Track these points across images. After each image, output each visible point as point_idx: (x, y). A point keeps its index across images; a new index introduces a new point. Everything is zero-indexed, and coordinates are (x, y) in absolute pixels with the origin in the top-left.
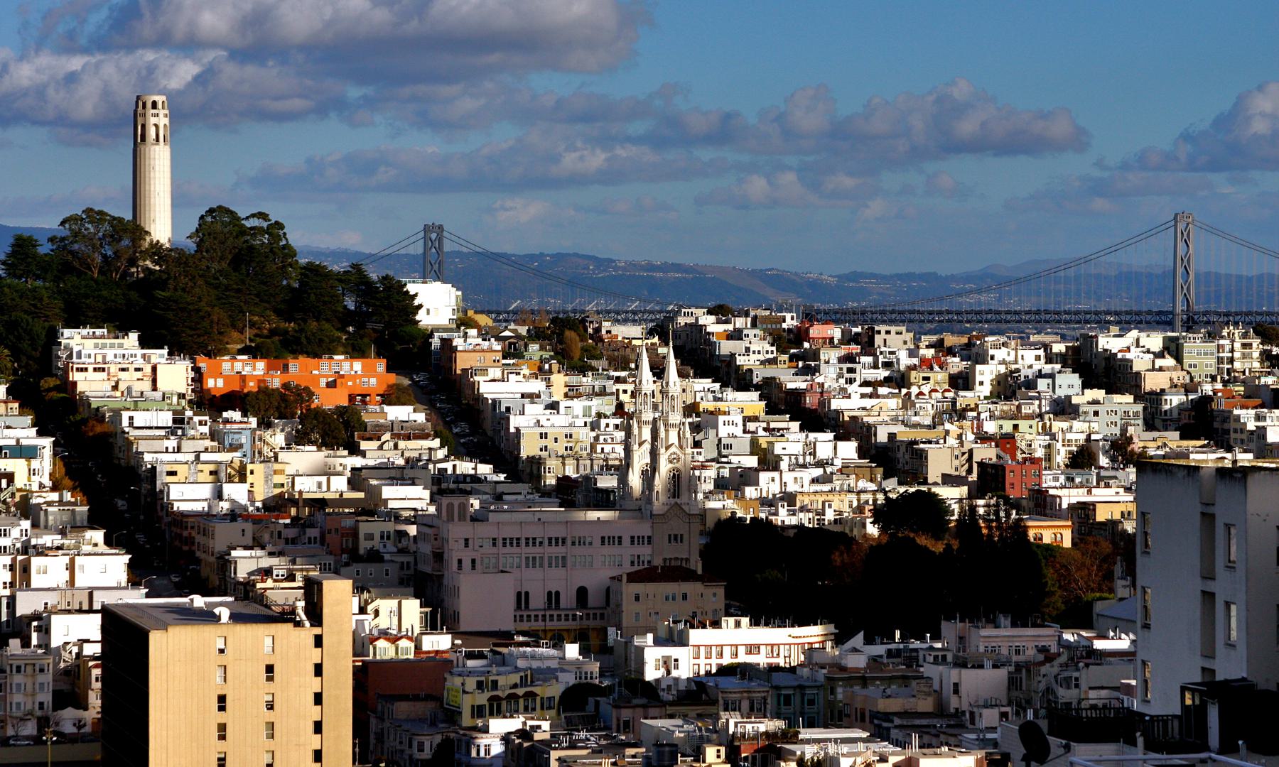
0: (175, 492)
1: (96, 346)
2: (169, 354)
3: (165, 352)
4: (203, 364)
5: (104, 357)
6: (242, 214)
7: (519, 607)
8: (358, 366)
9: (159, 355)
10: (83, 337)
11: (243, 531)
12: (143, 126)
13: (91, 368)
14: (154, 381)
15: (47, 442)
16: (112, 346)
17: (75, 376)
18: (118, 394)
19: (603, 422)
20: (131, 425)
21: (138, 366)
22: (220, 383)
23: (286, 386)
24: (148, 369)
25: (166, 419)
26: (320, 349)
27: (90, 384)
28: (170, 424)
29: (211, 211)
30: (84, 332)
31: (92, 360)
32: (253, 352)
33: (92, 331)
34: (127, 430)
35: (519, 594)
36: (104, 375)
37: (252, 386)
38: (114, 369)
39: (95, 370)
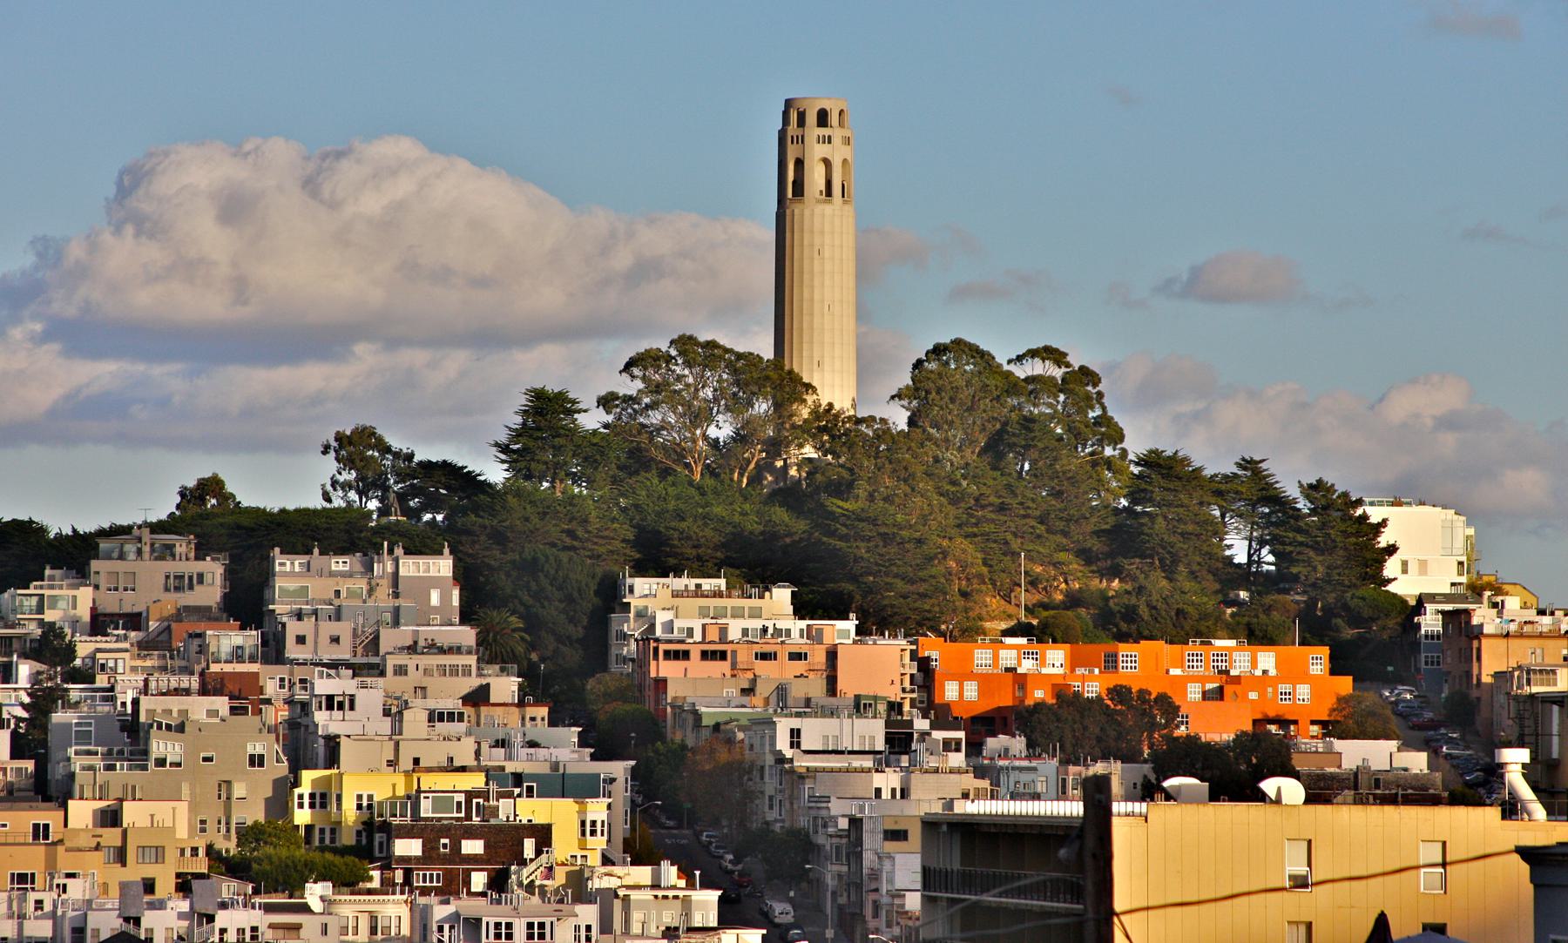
1: (704, 612)
2: (860, 631)
3: (850, 625)
5: (723, 631)
12: (799, 163)
13: (695, 654)
15: (619, 769)
16: (738, 614)
22: (971, 691)
24: (818, 657)
25: (874, 731)
28: (880, 745)
31: (698, 637)
33: (692, 583)
36: (724, 666)
38: (744, 656)
39: (705, 655)
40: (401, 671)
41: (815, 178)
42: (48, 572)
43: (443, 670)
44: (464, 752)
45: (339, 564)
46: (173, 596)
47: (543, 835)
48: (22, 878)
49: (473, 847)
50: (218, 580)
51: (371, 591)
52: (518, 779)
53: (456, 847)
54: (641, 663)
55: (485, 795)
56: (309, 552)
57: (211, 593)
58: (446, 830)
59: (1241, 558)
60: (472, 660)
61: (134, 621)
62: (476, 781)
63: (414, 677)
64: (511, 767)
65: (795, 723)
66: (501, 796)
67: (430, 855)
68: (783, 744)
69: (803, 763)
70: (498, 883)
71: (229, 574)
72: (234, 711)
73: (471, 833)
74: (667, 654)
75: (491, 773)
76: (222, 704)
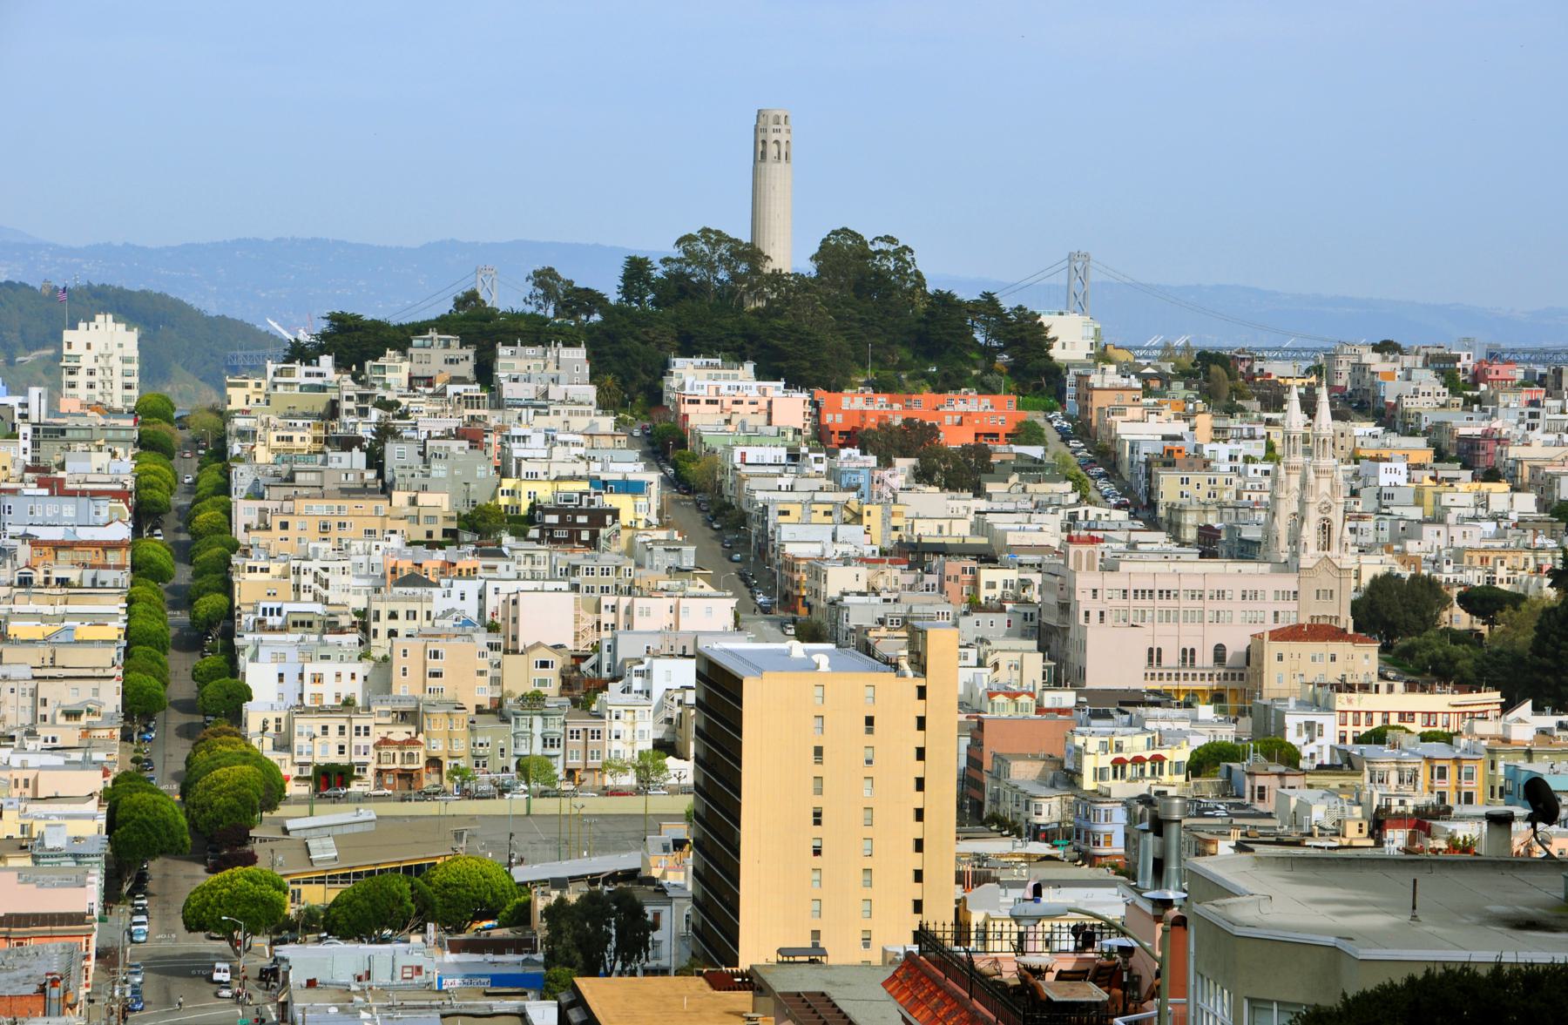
0: (786, 533)
1: (709, 377)
2: (786, 387)
3: (781, 384)
4: (820, 394)
5: (717, 389)
6: (868, 238)
7: (1151, 659)
8: (986, 401)
9: (775, 388)
10: (696, 367)
11: (462, 598)
12: (764, 142)
13: (703, 401)
14: (770, 415)
16: (726, 377)
17: (686, 409)
18: (730, 428)
19: (1251, 467)
20: (743, 461)
21: (752, 399)
22: (839, 418)
23: (908, 422)
24: (763, 404)
25: (782, 453)
26: (948, 383)
27: (700, 419)
28: (784, 461)
29: (835, 233)
30: (697, 361)
31: (704, 392)
32: (880, 386)
34: (738, 466)
35: (1151, 651)
36: (717, 408)
37: (872, 422)
38: (727, 403)
39: (708, 402)
40: (557, 413)
41: (772, 150)
42: (388, 352)
43: (577, 413)
44: (581, 469)
45: (529, 351)
46: (449, 367)
47: (615, 513)
48: (370, 532)
49: (582, 519)
50: (471, 358)
51: (545, 366)
52: (605, 483)
53: (574, 519)
54: (677, 404)
55: (588, 494)
56: (515, 344)
57: (467, 369)
58: (569, 511)
59: (981, 340)
60: (592, 408)
61: (429, 381)
62: (584, 486)
63: (564, 416)
64: (604, 477)
65: (743, 449)
66: (596, 494)
67: (562, 523)
68: (737, 459)
69: (746, 470)
70: (593, 543)
71: (476, 354)
72: (471, 447)
73: (582, 512)
74: (691, 402)
75: (592, 480)
76: (466, 444)
